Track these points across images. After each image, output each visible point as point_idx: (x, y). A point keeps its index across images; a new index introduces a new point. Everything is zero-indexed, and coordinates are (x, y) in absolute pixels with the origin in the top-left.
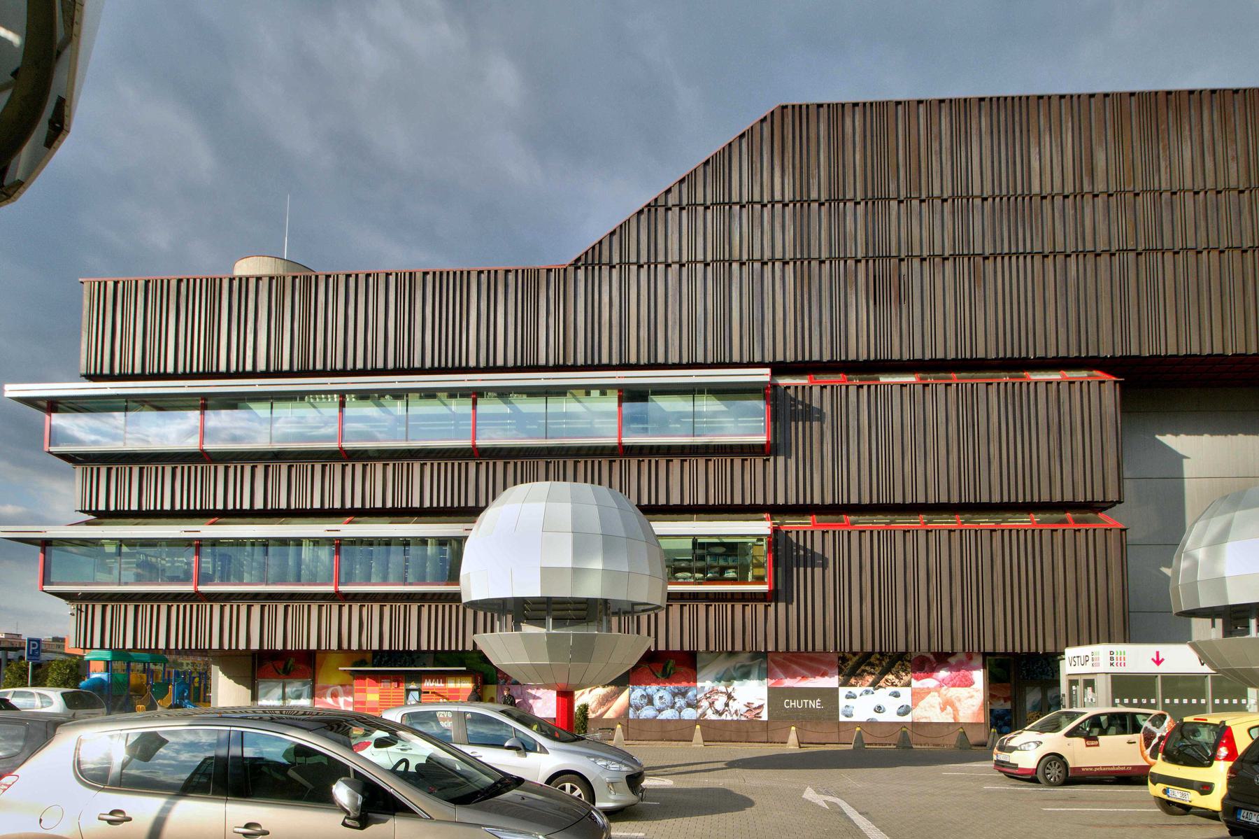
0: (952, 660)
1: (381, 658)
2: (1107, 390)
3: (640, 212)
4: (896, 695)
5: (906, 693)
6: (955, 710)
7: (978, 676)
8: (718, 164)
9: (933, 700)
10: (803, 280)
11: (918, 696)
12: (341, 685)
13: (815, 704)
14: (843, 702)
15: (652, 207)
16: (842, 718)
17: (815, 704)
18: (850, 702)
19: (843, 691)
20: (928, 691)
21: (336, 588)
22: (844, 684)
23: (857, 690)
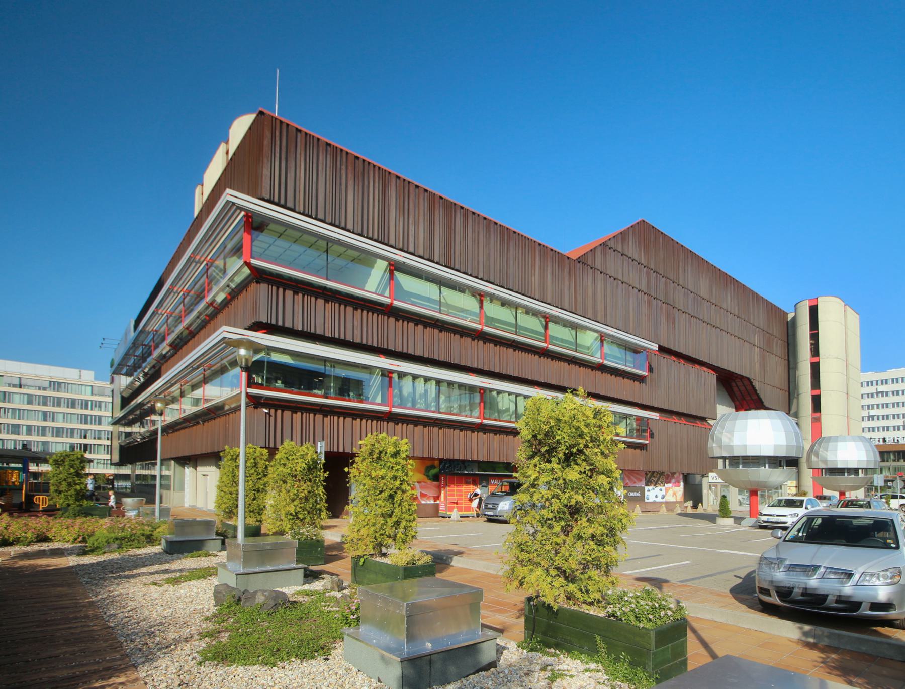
0: (675, 476)
1: (445, 465)
2: (712, 378)
3: (601, 245)
4: (661, 490)
5: (663, 488)
6: (676, 496)
7: (682, 484)
8: (623, 235)
9: (670, 492)
10: (649, 303)
11: (667, 490)
12: (418, 482)
13: (638, 494)
14: (646, 493)
15: (604, 245)
16: (646, 500)
17: (638, 494)
18: (648, 493)
19: (647, 488)
20: (669, 488)
21: (390, 408)
22: (647, 485)
23: (650, 488)
